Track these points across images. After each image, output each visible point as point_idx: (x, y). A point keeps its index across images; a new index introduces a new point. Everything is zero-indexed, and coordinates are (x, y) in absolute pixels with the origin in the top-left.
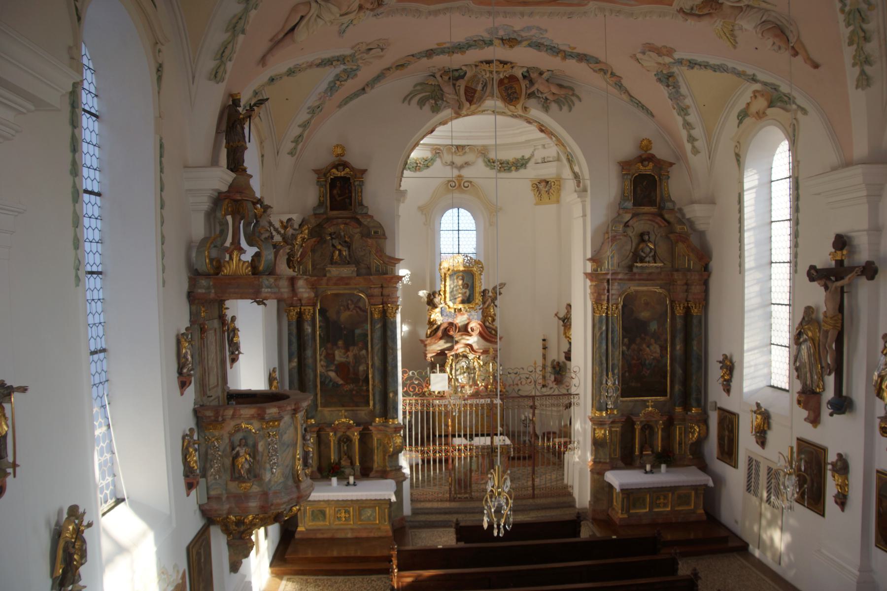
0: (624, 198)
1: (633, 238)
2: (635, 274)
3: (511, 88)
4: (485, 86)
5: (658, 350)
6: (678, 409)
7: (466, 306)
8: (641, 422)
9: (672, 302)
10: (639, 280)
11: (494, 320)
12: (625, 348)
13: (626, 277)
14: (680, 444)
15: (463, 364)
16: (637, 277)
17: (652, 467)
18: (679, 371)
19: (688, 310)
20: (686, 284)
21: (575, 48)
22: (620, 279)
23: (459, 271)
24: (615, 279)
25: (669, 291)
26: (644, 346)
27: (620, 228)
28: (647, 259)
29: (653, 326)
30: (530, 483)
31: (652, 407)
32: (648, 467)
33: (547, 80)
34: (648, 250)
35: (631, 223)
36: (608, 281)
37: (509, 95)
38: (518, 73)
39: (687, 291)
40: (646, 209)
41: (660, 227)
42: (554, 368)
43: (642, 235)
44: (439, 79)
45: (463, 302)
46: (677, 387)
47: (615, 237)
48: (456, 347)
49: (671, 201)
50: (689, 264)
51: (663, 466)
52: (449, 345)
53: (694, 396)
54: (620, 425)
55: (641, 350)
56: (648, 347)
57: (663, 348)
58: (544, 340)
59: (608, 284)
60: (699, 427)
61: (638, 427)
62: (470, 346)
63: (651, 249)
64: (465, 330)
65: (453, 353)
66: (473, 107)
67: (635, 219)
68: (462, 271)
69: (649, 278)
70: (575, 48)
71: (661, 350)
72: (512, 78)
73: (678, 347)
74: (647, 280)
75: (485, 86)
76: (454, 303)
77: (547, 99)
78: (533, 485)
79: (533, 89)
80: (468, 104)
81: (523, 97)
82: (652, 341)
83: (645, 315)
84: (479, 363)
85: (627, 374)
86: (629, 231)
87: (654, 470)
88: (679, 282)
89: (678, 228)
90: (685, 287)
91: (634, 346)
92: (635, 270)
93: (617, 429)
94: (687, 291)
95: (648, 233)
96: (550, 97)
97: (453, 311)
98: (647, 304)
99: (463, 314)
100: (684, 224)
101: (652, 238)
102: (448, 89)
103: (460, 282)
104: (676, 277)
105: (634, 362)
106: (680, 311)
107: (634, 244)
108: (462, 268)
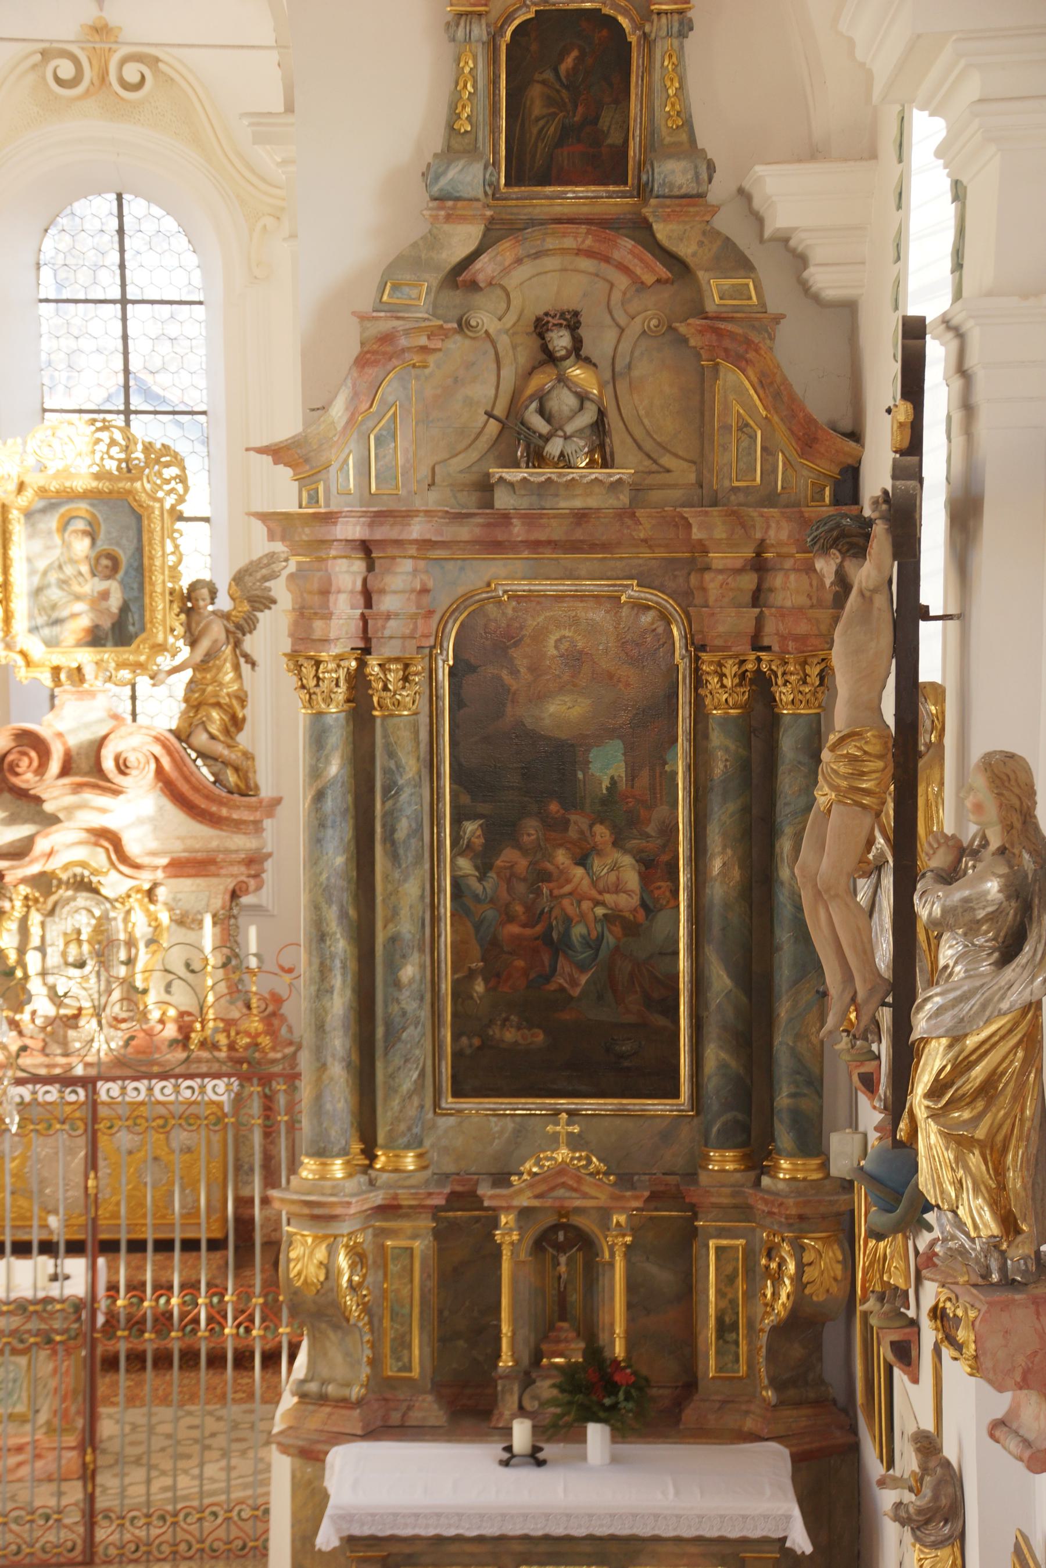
0: (456, 144)
1: (504, 342)
2: (505, 518)
5: (632, 879)
6: (723, 1162)
7: (109, 655)
8: (525, 1213)
9: (698, 647)
10: (535, 545)
11: (236, 723)
12: (465, 865)
13: (464, 532)
14: (725, 1328)
15: (79, 916)
16: (518, 531)
17: (543, 1432)
18: (721, 980)
19: (761, 685)
20: (759, 565)
22: (425, 544)
23: (70, 496)
24: (398, 543)
25: (685, 598)
26: (562, 857)
27: (421, 296)
28: (554, 447)
29: (607, 766)
30: (75, 1493)
31: (575, 1142)
32: (521, 1433)
34: (571, 401)
35: (485, 267)
36: (366, 548)
39: (758, 598)
40: (575, 197)
41: (640, 286)
43: (541, 327)
45: (95, 638)
46: (714, 1055)
47: (387, 338)
48: (41, 845)
49: (690, 149)
50: (769, 472)
51: (596, 1433)
52: (24, 830)
53: (783, 1100)
54: (426, 1223)
55: (545, 876)
56: (582, 861)
57: (657, 868)
59: (370, 568)
60: (799, 1250)
61: (508, 1232)
62: (109, 839)
63: (583, 398)
64: (88, 767)
65: (35, 869)
67: (506, 251)
68: (87, 495)
69: (580, 539)
71: (645, 879)
73: (716, 865)
74: (573, 547)
76: (51, 643)
78: (91, 1498)
82: (602, 833)
83: (562, 711)
84: (153, 918)
85: (479, 987)
86: (485, 317)
87: (549, 1450)
88: (717, 558)
89: (716, 290)
90: (748, 581)
91: (509, 856)
92: (503, 500)
93: (417, 1240)
94: (758, 598)
95: (572, 322)
97: (46, 679)
98: (576, 659)
99: (92, 694)
100: (744, 265)
101: (600, 342)
103: (82, 546)
104: (696, 534)
105: (514, 929)
106: (724, 698)
107: (509, 375)
108: (82, 483)
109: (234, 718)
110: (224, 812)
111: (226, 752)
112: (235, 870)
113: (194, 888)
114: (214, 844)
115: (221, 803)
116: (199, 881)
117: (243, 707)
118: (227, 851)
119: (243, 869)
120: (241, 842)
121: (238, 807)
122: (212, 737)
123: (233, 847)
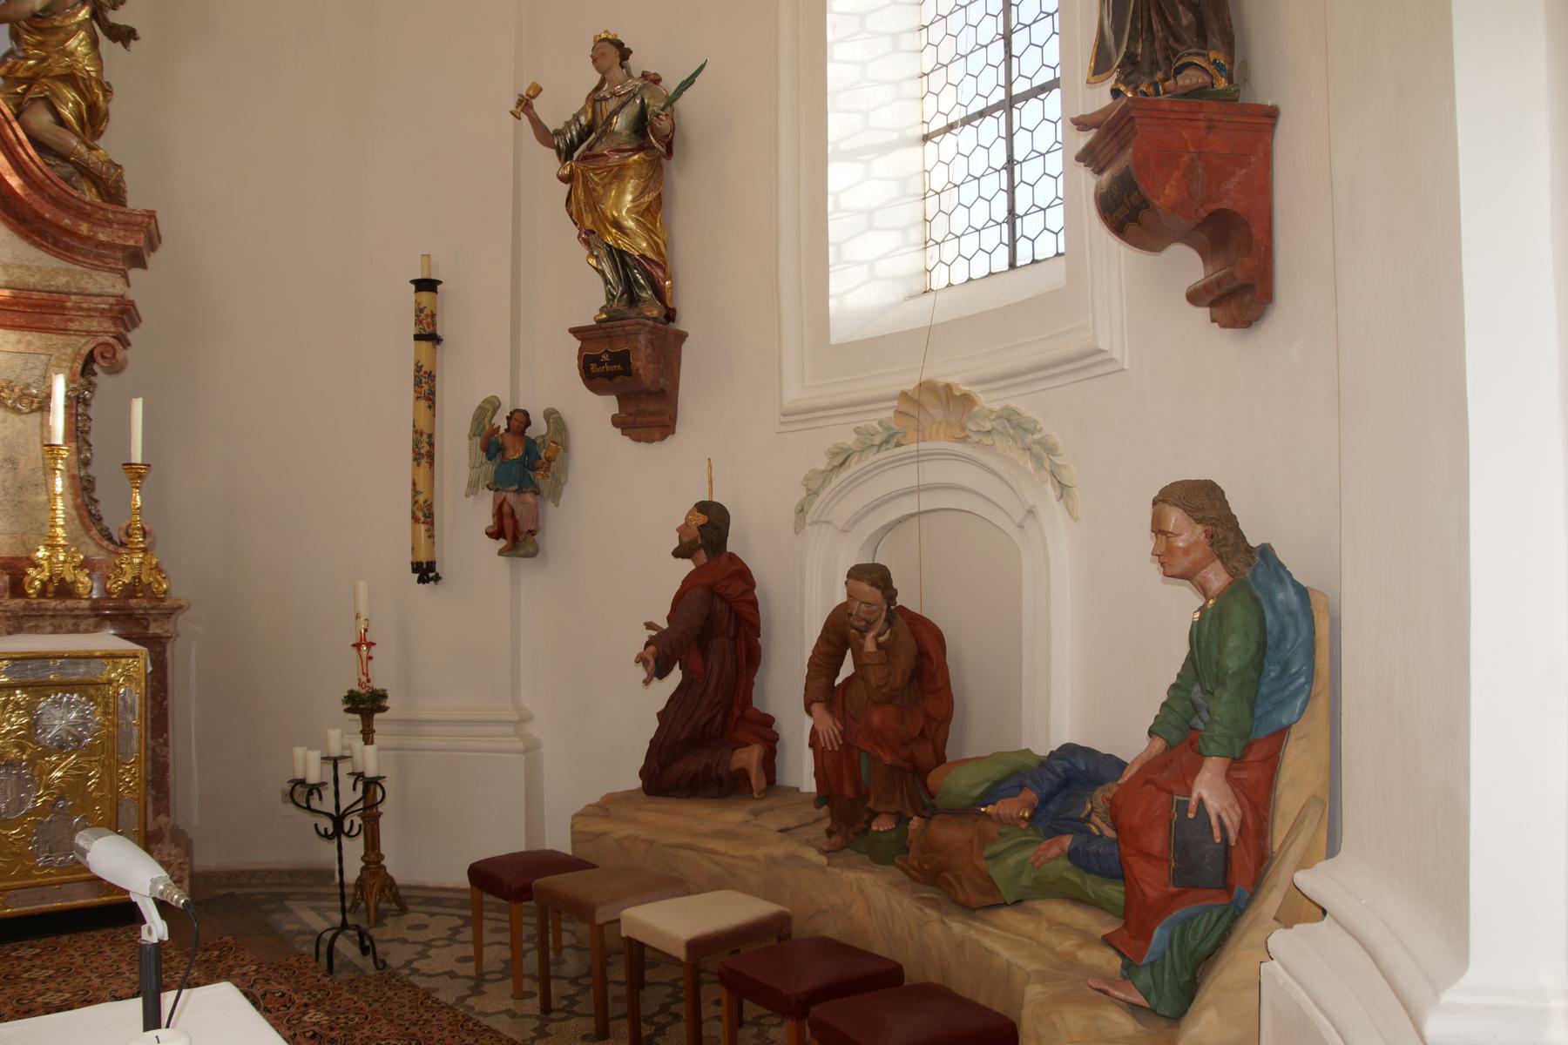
11: (93, 120)
42: (491, 446)
58: (426, 285)
109: (93, 108)
110: (84, 228)
111: (82, 149)
112: (94, 325)
113: (22, 348)
114: (61, 281)
115: (81, 213)
116: (30, 337)
117: (107, 101)
118: (83, 293)
119: (108, 325)
120: (104, 283)
121: (110, 223)
122: (60, 121)
123: (93, 289)
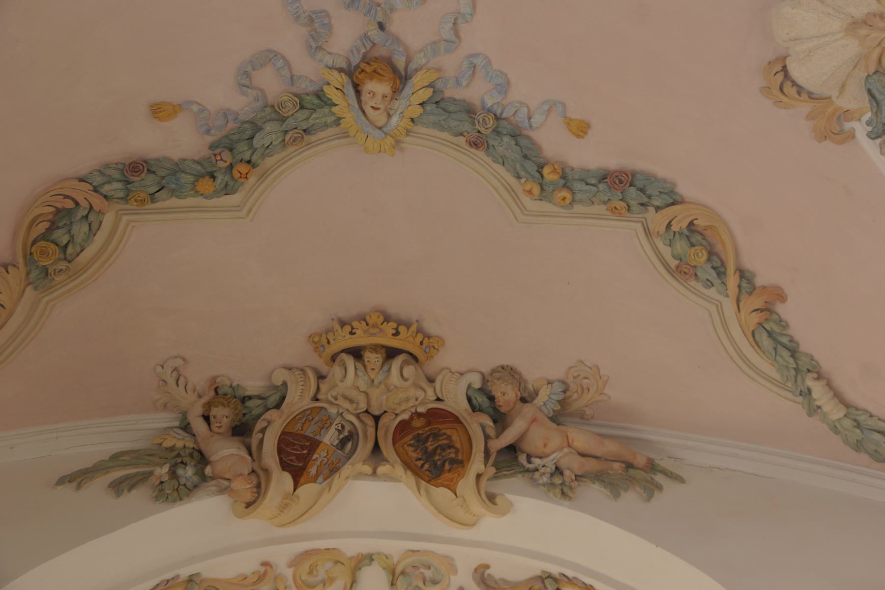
3: (436, 436)
4: (348, 439)
21: (581, 129)
33: (556, 419)
37: (428, 456)
38: (456, 402)
44: (199, 426)
66: (307, 490)
70: (581, 129)
72: (438, 417)
75: (348, 439)
77: (558, 471)
79: (509, 437)
80: (287, 479)
81: (477, 464)
96: (572, 464)
102: (226, 453)
